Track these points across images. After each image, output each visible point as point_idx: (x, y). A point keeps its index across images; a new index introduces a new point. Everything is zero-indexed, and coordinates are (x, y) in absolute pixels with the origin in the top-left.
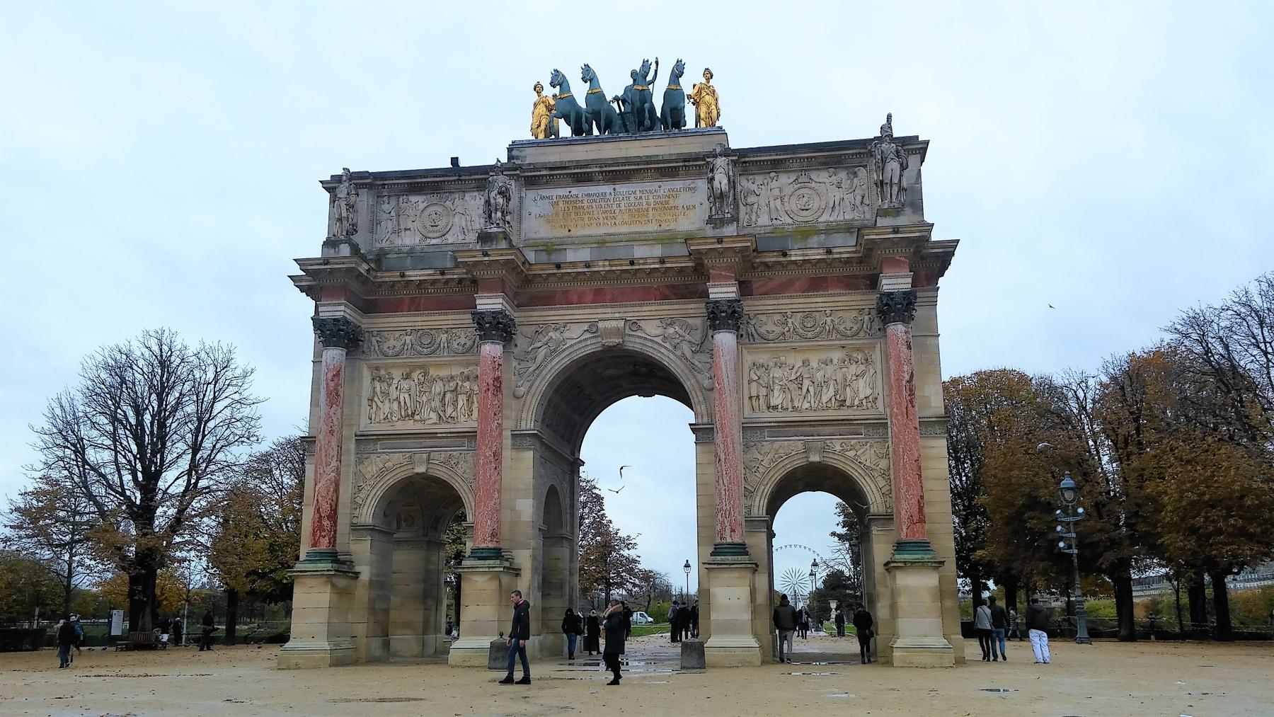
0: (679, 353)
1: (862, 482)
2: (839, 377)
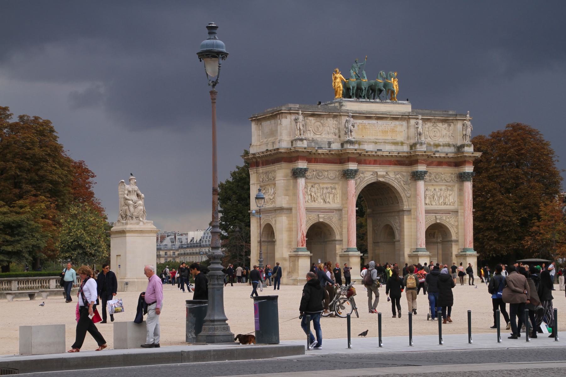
0: (400, 184)
1: (450, 229)
2: (445, 195)
